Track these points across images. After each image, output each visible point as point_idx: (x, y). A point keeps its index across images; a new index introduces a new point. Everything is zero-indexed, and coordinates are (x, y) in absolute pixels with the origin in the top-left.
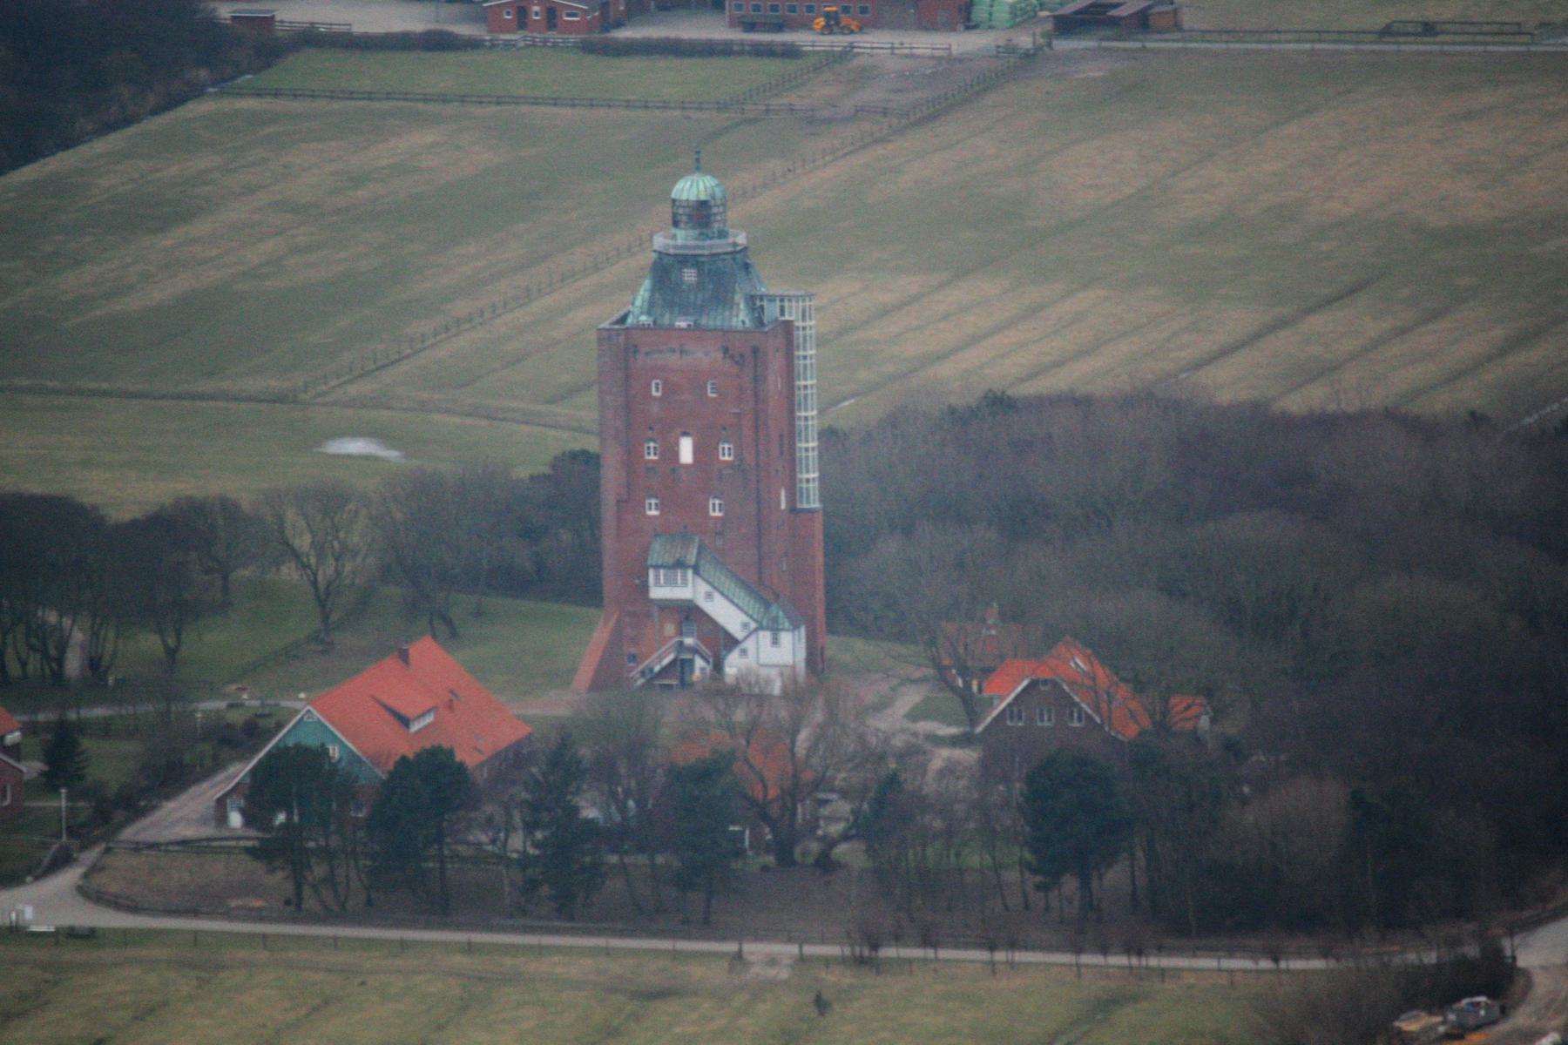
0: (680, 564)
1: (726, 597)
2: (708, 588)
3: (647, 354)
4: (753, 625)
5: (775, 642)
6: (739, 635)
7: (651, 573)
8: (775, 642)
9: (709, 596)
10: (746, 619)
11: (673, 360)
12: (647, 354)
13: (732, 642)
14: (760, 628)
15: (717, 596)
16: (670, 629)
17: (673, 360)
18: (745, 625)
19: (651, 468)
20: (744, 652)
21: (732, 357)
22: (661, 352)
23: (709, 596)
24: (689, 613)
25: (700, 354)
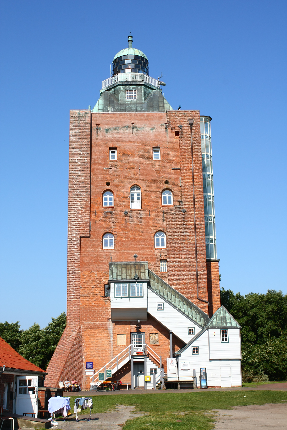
0: (138, 280)
1: (175, 307)
2: (161, 300)
3: (107, 130)
5: (224, 339)
7: (112, 285)
8: (224, 339)
9: (160, 307)
11: (127, 134)
12: (107, 130)
14: (205, 328)
15: (166, 306)
17: (127, 134)
20: (196, 350)
21: (173, 129)
22: (117, 128)
23: (160, 307)
25: (147, 129)
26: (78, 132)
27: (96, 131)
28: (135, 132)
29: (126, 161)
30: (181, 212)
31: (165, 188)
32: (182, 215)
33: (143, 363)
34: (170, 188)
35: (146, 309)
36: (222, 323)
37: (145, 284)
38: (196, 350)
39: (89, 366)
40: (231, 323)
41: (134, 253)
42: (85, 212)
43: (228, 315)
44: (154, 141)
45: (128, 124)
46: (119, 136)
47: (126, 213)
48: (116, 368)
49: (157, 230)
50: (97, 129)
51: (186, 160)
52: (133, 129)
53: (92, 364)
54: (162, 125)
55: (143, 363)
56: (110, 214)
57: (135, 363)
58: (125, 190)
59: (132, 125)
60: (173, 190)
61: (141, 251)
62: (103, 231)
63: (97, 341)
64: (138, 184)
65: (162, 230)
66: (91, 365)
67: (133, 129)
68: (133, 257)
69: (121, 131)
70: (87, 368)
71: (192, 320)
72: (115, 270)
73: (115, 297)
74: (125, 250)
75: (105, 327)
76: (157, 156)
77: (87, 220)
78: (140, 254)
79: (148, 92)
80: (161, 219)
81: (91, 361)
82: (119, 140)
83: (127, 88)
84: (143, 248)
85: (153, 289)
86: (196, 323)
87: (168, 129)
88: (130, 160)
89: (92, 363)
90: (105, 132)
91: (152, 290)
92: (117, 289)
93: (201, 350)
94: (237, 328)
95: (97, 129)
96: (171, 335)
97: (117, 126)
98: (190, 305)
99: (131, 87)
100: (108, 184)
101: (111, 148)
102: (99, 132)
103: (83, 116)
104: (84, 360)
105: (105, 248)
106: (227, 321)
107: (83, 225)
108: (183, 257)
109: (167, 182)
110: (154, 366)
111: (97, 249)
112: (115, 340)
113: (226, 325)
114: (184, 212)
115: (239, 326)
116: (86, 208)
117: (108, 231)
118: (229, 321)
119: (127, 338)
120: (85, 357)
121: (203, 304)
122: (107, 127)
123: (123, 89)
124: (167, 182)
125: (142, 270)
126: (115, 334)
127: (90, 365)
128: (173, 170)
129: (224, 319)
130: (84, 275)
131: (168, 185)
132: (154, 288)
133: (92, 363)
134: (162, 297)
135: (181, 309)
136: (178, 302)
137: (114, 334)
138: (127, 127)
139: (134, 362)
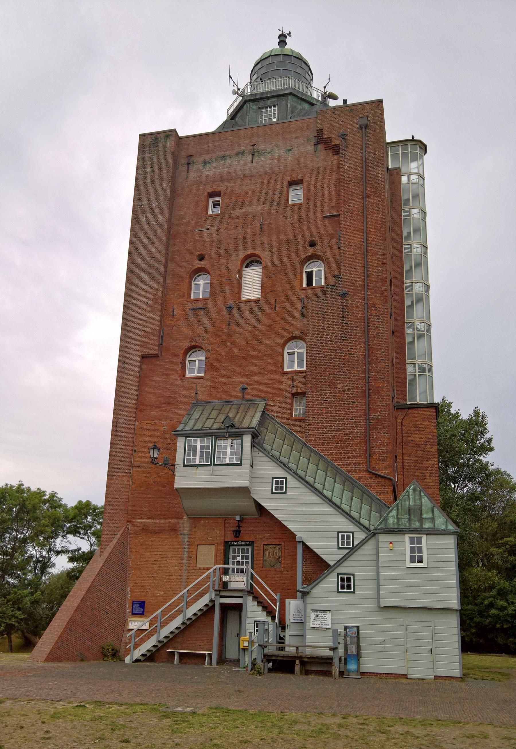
0: (231, 431)
1: (311, 486)
2: (279, 472)
3: (205, 163)
4: (360, 536)
6: (330, 556)
7: (180, 442)
9: (279, 487)
10: (347, 526)
13: (318, 566)
15: (293, 485)
16: (207, 556)
18: (343, 537)
19: (198, 309)
20: (346, 583)
22: (223, 158)
23: (279, 487)
24: (247, 525)
25: (280, 152)
26: (150, 169)
27: (186, 168)
28: (256, 159)
29: (238, 212)
30: (338, 297)
31: (309, 254)
32: (339, 300)
33: (239, 608)
34: (319, 253)
35: (245, 491)
36: (410, 519)
37: (247, 439)
38: (346, 583)
39: (137, 609)
40: (433, 520)
41: (241, 382)
42: (153, 310)
43: (425, 500)
44: (292, 170)
45: (243, 148)
46: (225, 170)
47: (230, 309)
48: (181, 615)
49: (289, 336)
50: (188, 164)
51: (352, 196)
52: (253, 155)
53: (142, 604)
54: (307, 141)
55: (239, 608)
56: (201, 312)
57: (225, 608)
58: (230, 266)
59: (252, 147)
60: (325, 257)
61: (255, 379)
62: (186, 344)
63: (157, 557)
64: (256, 252)
65: (299, 334)
66: (140, 609)
67: (253, 155)
68: (238, 389)
69: (231, 161)
70: (133, 614)
71: (348, 515)
72: (196, 415)
73: (185, 466)
74: (222, 377)
75: (174, 530)
76: (296, 196)
77: (156, 326)
78: (251, 384)
79: (300, 107)
80: (297, 314)
81: (142, 599)
82: (224, 178)
83: (262, 104)
84: (259, 373)
85: (265, 450)
86: (357, 523)
87: (319, 146)
88: (243, 210)
89: (144, 602)
90: (201, 167)
91: (264, 451)
92: (189, 449)
93: (359, 582)
94: (445, 533)
95: (188, 164)
96: (300, 548)
97: (224, 153)
98: (349, 483)
99: (269, 103)
100: (201, 258)
101: (211, 195)
102: (190, 169)
103: (160, 142)
104: (129, 596)
105: (188, 375)
106: (424, 516)
107: (146, 334)
108: (339, 386)
109: (312, 244)
110: (262, 616)
111: (172, 377)
112: (193, 557)
113: (421, 525)
114: (344, 295)
115: (451, 527)
116: (155, 303)
117: (194, 343)
118: (430, 515)
119: (216, 552)
120: (130, 591)
121: (380, 482)
122: (206, 157)
123: (255, 107)
124: (312, 244)
125: (250, 414)
126: (193, 546)
127: (140, 606)
128: (326, 221)
129: (415, 511)
130: (142, 427)
131: (314, 249)
132: (268, 448)
133: (144, 602)
134: (285, 466)
135: (325, 492)
136: (320, 477)
137: (190, 543)
138: (241, 153)
139: (221, 604)
